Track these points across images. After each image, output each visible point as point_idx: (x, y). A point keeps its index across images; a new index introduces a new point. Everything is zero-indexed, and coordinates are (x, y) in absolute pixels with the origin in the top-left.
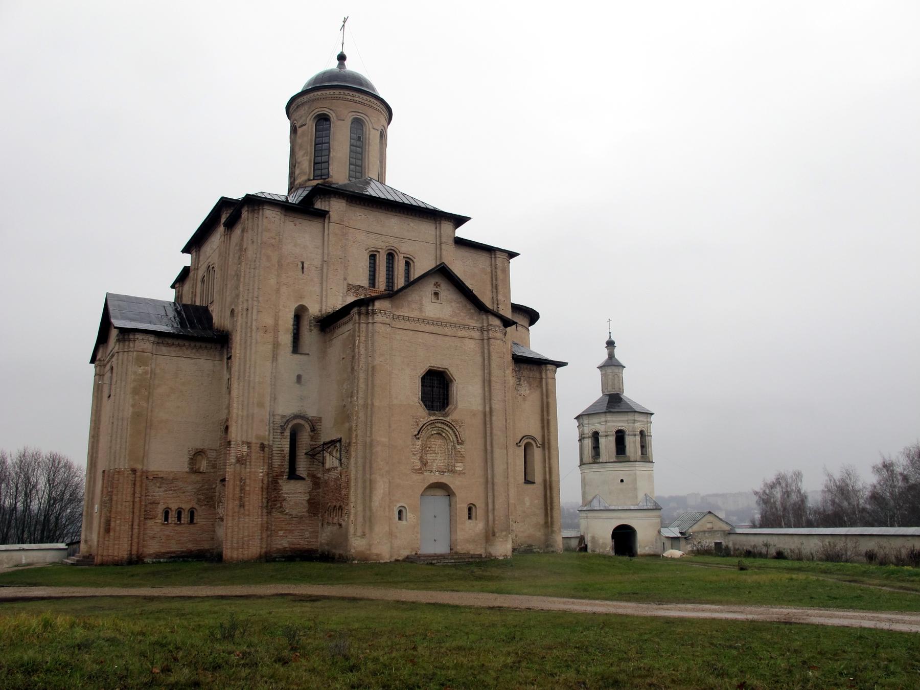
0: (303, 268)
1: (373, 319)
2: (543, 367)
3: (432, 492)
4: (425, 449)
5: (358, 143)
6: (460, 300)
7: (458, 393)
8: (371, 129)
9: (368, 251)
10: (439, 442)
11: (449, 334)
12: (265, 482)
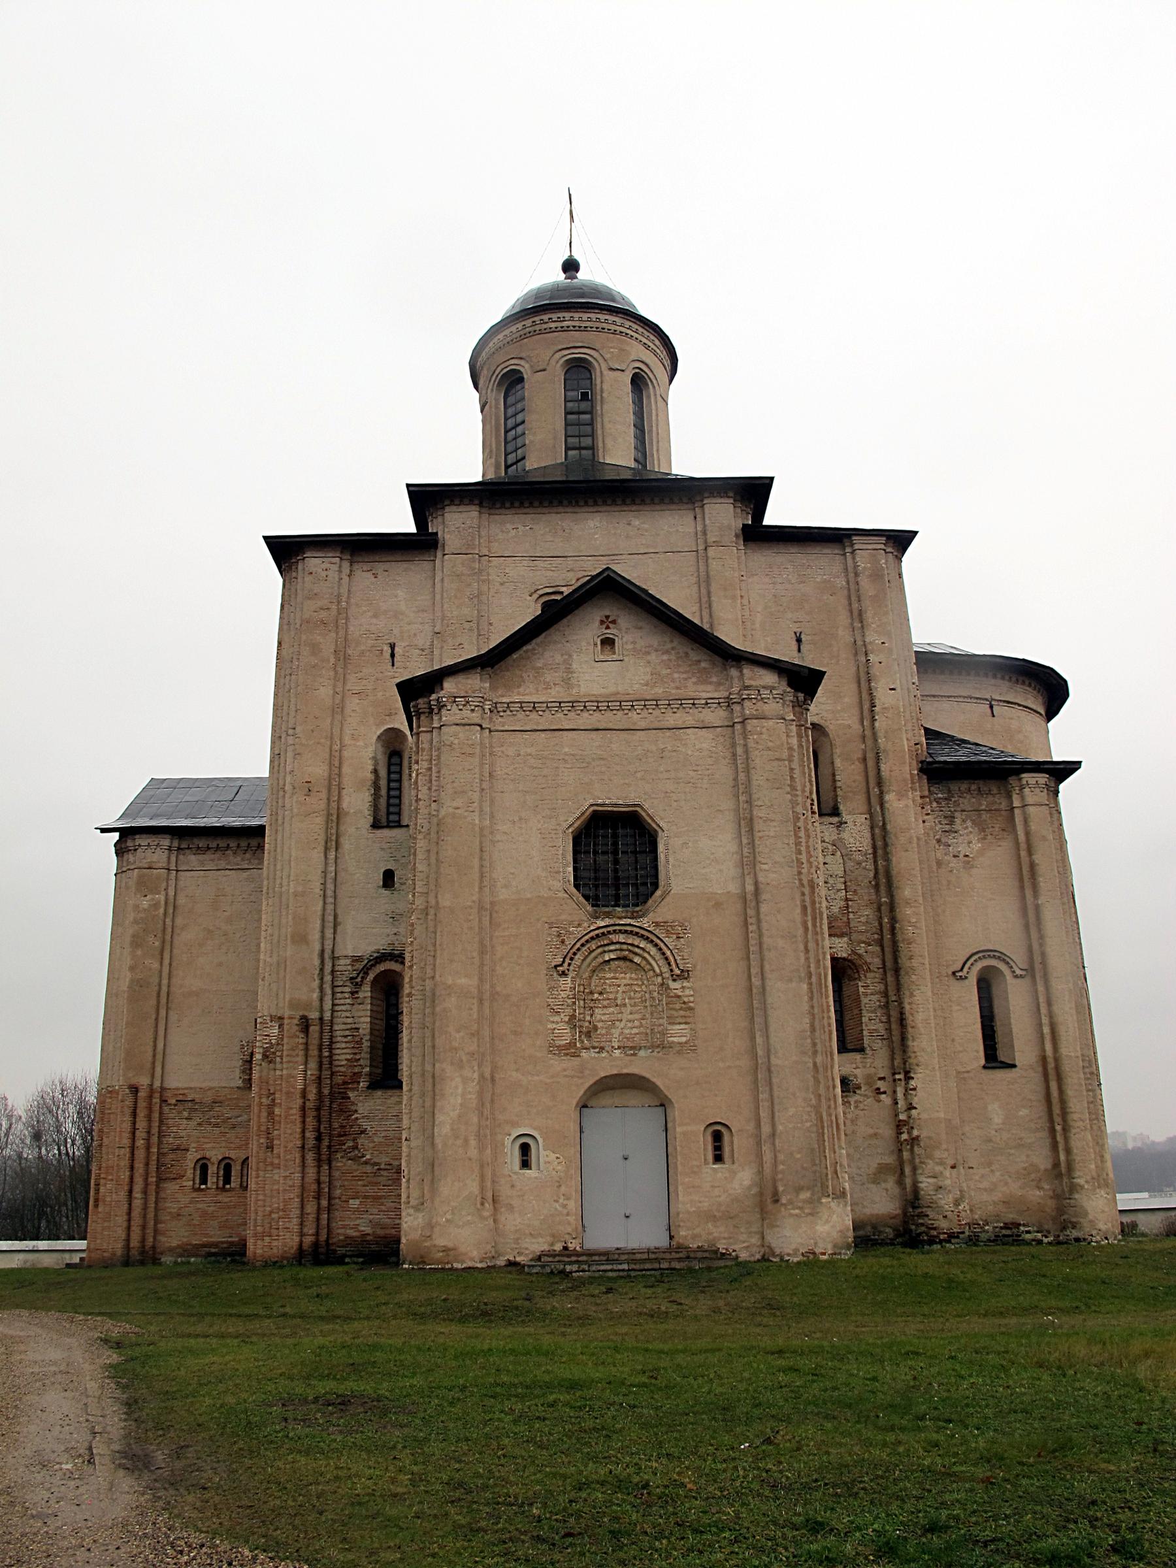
0: (393, 655)
1: (440, 719)
2: (1012, 780)
3: (607, 1099)
4: (586, 997)
5: (584, 406)
6: (669, 646)
7: (671, 860)
8: (606, 372)
9: (535, 596)
10: (627, 978)
11: (643, 725)
12: (312, 1095)
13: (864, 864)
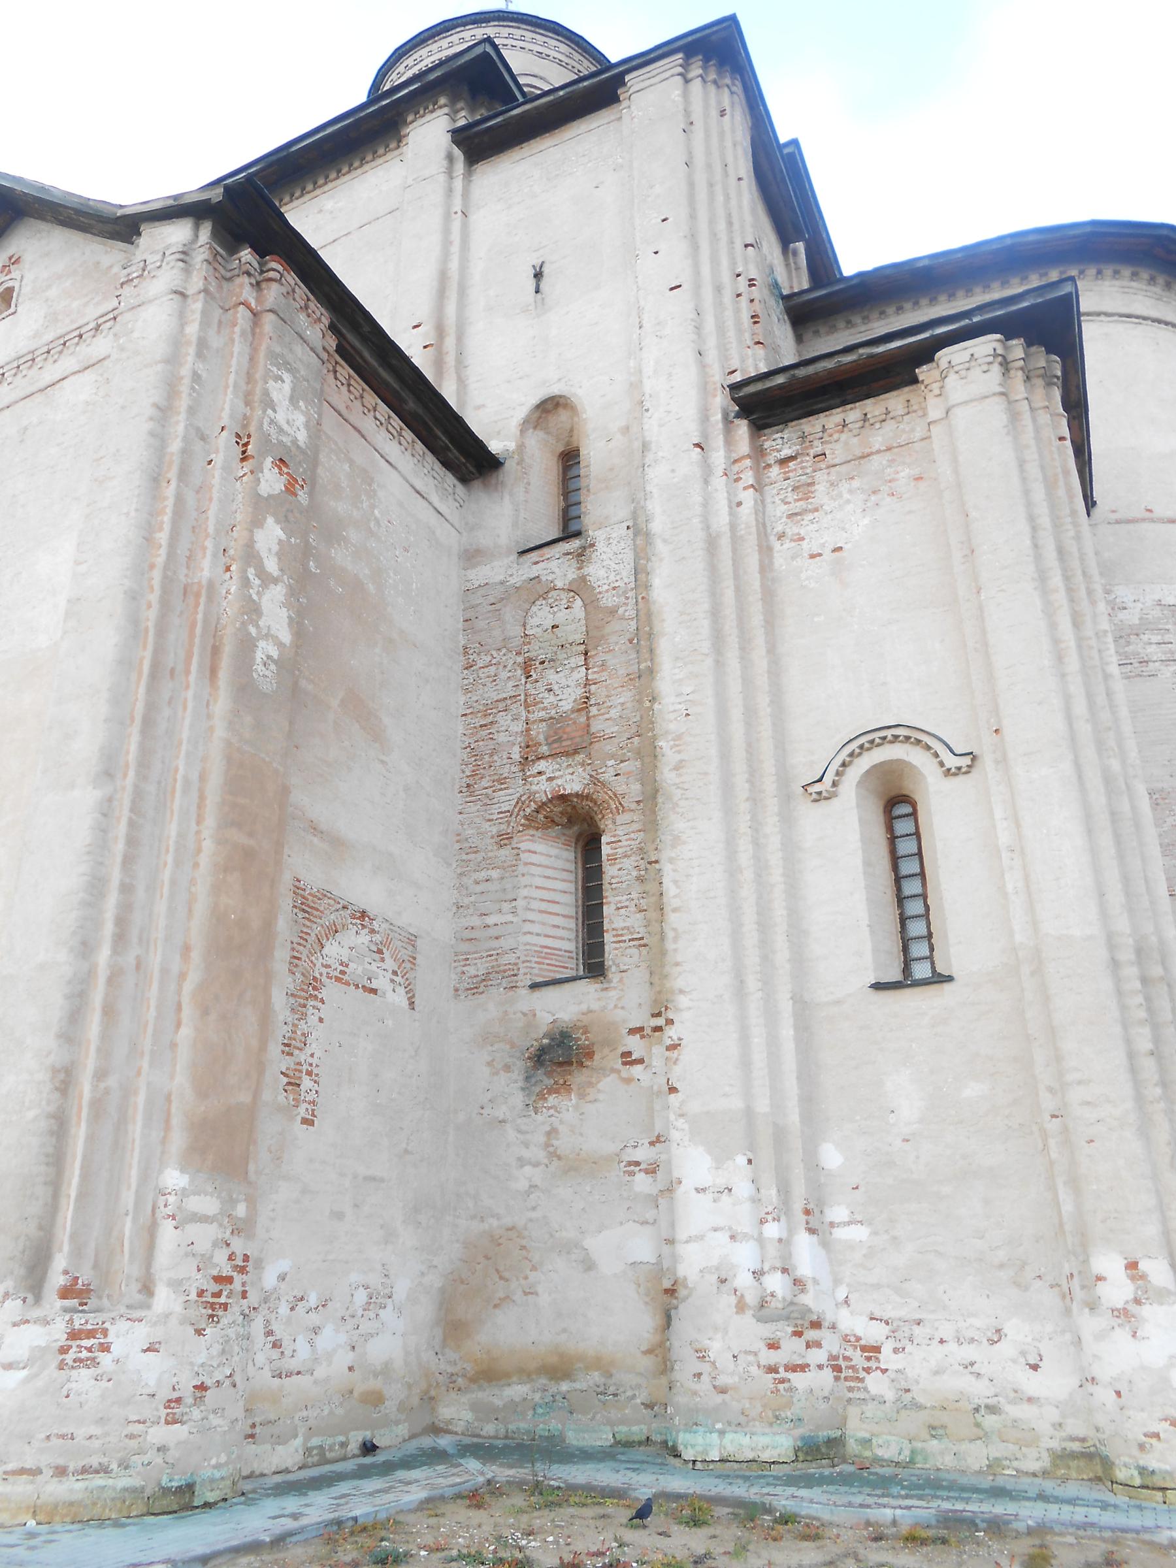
13: (621, 611)
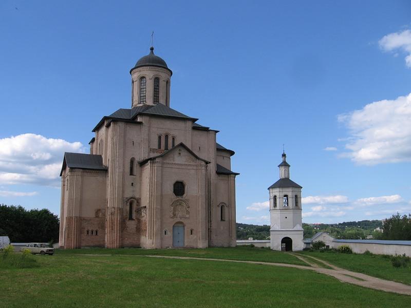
4: (175, 210)
5: (158, 88)
10: (180, 207)
